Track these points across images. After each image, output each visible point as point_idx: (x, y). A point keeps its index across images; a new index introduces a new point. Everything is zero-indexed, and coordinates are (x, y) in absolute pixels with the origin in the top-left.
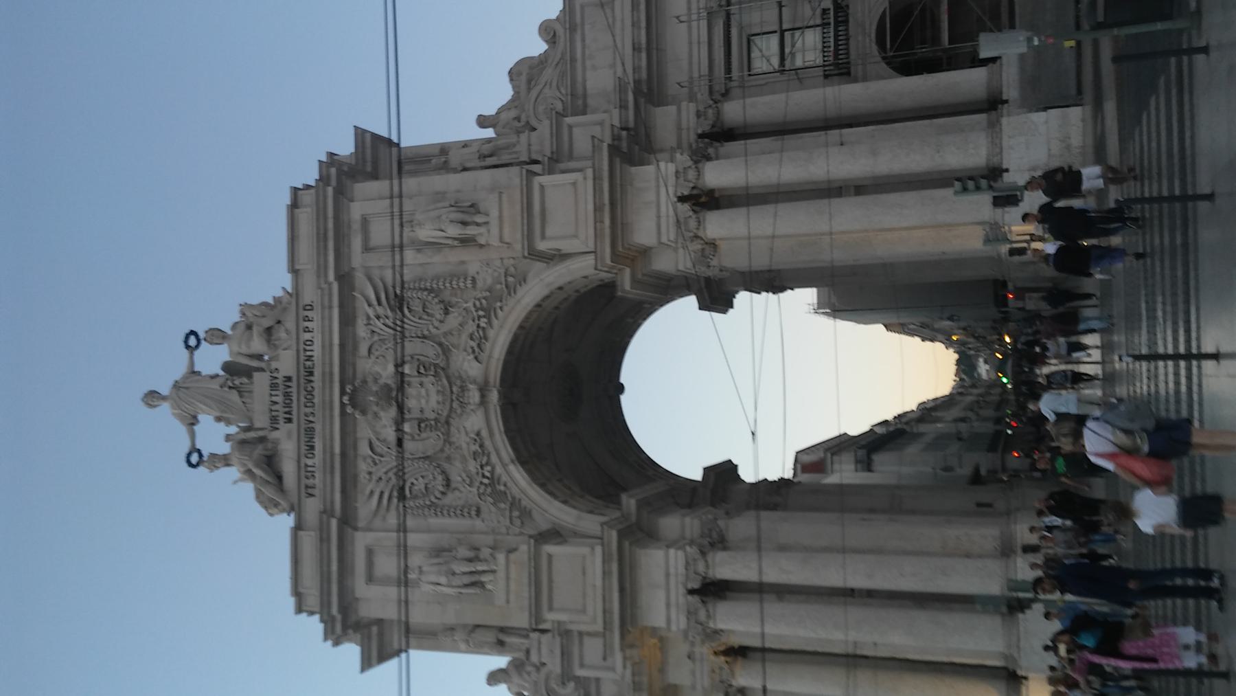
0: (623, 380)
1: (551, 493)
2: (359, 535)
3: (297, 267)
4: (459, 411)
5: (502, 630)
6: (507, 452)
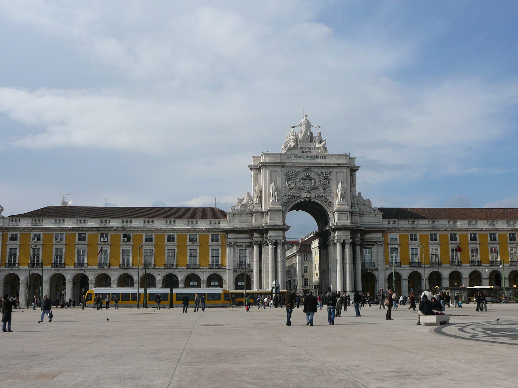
5: (260, 198)
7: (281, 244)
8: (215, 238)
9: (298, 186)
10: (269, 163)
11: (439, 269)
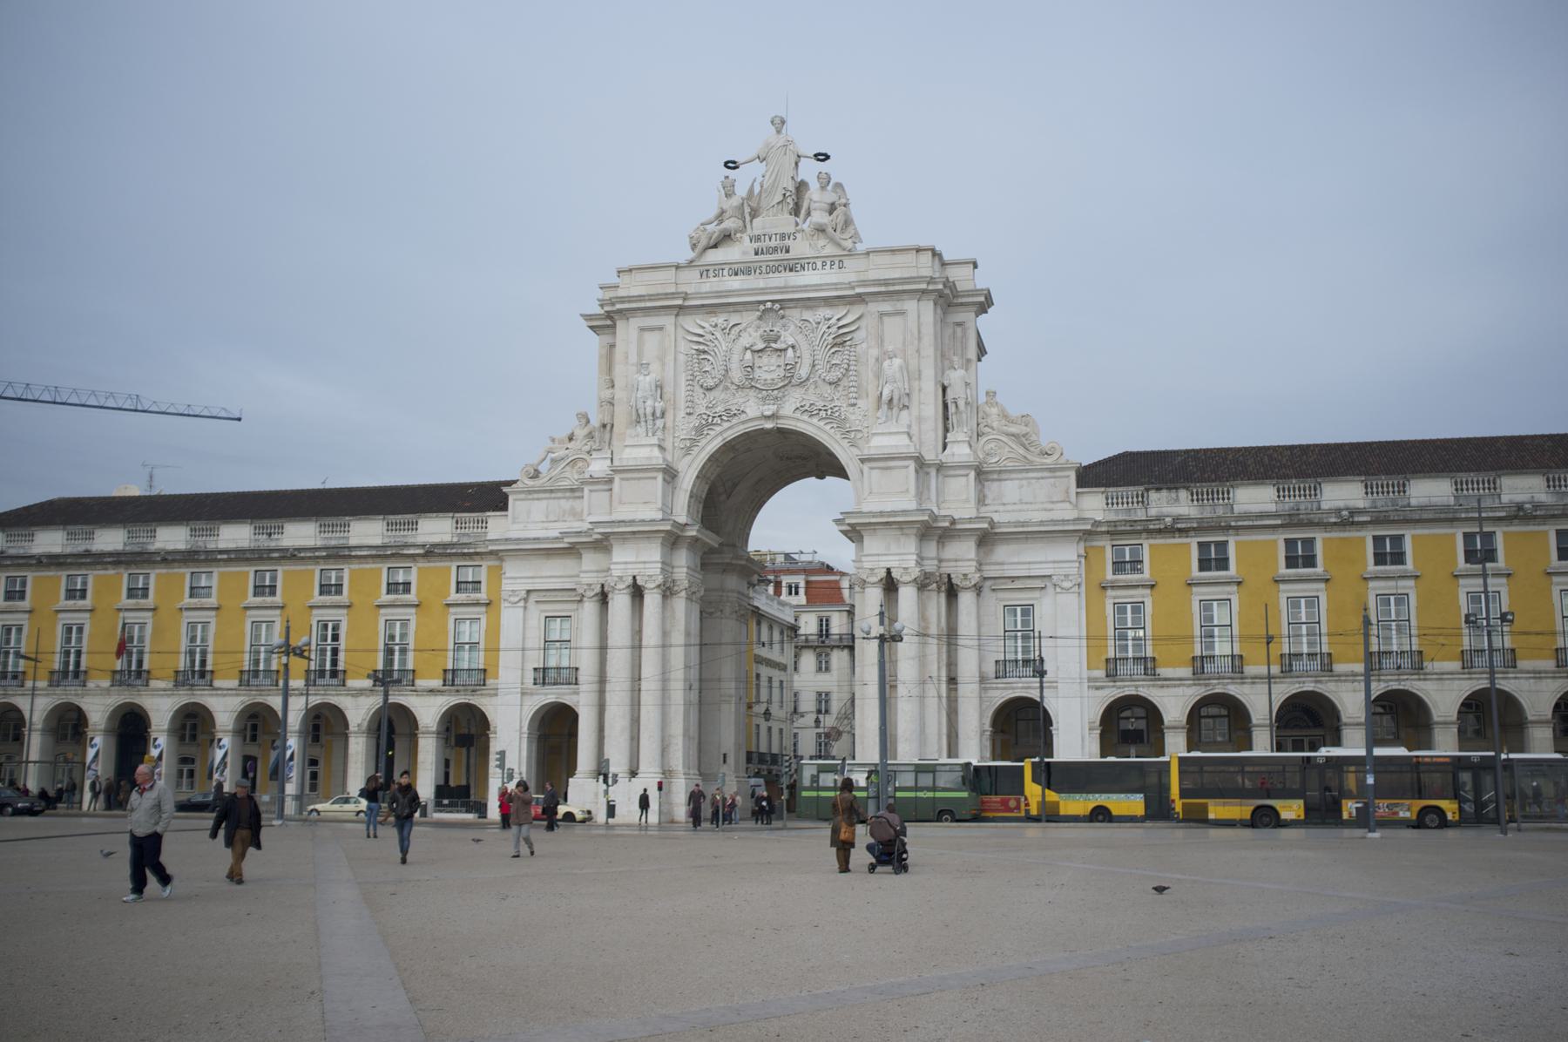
0: (829, 479)
1: (703, 467)
2: (673, 317)
3: (871, 254)
4: (760, 396)
5: (612, 426)
6: (731, 435)
7: (655, 591)
8: (470, 579)
9: (737, 375)
10: (630, 299)
11: (1320, 682)
